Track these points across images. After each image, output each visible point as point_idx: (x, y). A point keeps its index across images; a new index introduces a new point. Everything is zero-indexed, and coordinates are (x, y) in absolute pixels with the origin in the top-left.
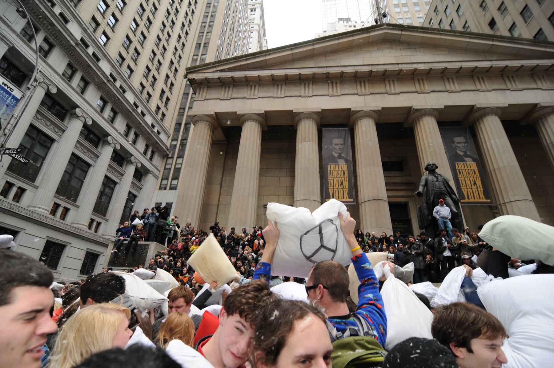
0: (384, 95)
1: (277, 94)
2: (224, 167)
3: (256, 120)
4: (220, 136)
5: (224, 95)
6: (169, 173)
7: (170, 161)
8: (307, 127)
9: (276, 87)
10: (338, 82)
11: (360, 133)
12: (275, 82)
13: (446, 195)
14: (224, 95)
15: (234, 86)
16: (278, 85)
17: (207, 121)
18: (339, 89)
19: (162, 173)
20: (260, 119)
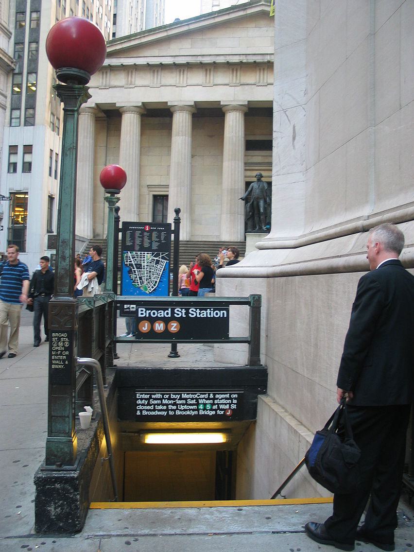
0: (253, 86)
1: (153, 83)
2: (107, 146)
3: (135, 112)
4: (102, 115)
5: (102, 83)
6: (20, 100)
7: (17, 79)
8: (181, 120)
9: (152, 74)
10: (212, 69)
11: (228, 127)
12: (150, 68)
13: (261, 199)
14: (102, 83)
15: (111, 70)
16: (154, 71)
17: (89, 112)
18: (212, 78)
19: (9, 99)
20: (138, 109)
